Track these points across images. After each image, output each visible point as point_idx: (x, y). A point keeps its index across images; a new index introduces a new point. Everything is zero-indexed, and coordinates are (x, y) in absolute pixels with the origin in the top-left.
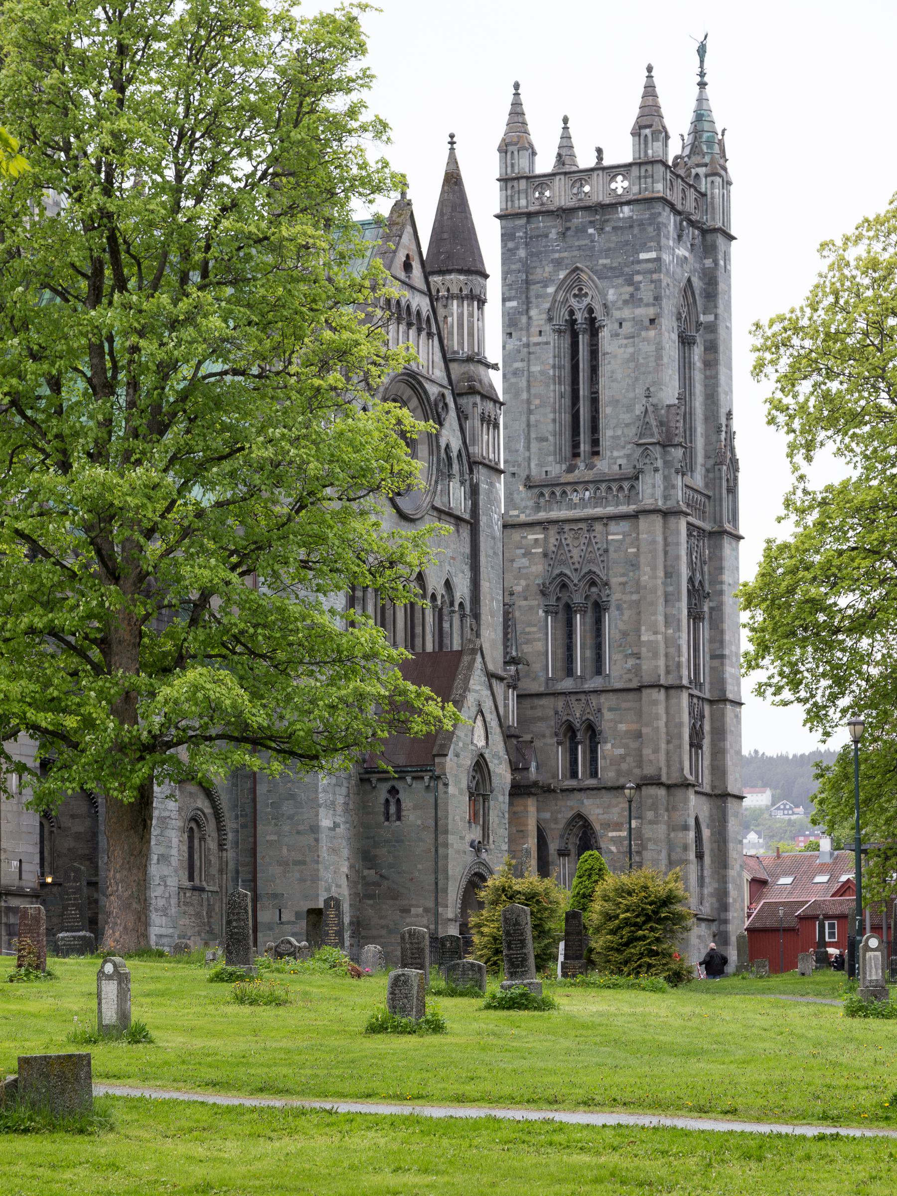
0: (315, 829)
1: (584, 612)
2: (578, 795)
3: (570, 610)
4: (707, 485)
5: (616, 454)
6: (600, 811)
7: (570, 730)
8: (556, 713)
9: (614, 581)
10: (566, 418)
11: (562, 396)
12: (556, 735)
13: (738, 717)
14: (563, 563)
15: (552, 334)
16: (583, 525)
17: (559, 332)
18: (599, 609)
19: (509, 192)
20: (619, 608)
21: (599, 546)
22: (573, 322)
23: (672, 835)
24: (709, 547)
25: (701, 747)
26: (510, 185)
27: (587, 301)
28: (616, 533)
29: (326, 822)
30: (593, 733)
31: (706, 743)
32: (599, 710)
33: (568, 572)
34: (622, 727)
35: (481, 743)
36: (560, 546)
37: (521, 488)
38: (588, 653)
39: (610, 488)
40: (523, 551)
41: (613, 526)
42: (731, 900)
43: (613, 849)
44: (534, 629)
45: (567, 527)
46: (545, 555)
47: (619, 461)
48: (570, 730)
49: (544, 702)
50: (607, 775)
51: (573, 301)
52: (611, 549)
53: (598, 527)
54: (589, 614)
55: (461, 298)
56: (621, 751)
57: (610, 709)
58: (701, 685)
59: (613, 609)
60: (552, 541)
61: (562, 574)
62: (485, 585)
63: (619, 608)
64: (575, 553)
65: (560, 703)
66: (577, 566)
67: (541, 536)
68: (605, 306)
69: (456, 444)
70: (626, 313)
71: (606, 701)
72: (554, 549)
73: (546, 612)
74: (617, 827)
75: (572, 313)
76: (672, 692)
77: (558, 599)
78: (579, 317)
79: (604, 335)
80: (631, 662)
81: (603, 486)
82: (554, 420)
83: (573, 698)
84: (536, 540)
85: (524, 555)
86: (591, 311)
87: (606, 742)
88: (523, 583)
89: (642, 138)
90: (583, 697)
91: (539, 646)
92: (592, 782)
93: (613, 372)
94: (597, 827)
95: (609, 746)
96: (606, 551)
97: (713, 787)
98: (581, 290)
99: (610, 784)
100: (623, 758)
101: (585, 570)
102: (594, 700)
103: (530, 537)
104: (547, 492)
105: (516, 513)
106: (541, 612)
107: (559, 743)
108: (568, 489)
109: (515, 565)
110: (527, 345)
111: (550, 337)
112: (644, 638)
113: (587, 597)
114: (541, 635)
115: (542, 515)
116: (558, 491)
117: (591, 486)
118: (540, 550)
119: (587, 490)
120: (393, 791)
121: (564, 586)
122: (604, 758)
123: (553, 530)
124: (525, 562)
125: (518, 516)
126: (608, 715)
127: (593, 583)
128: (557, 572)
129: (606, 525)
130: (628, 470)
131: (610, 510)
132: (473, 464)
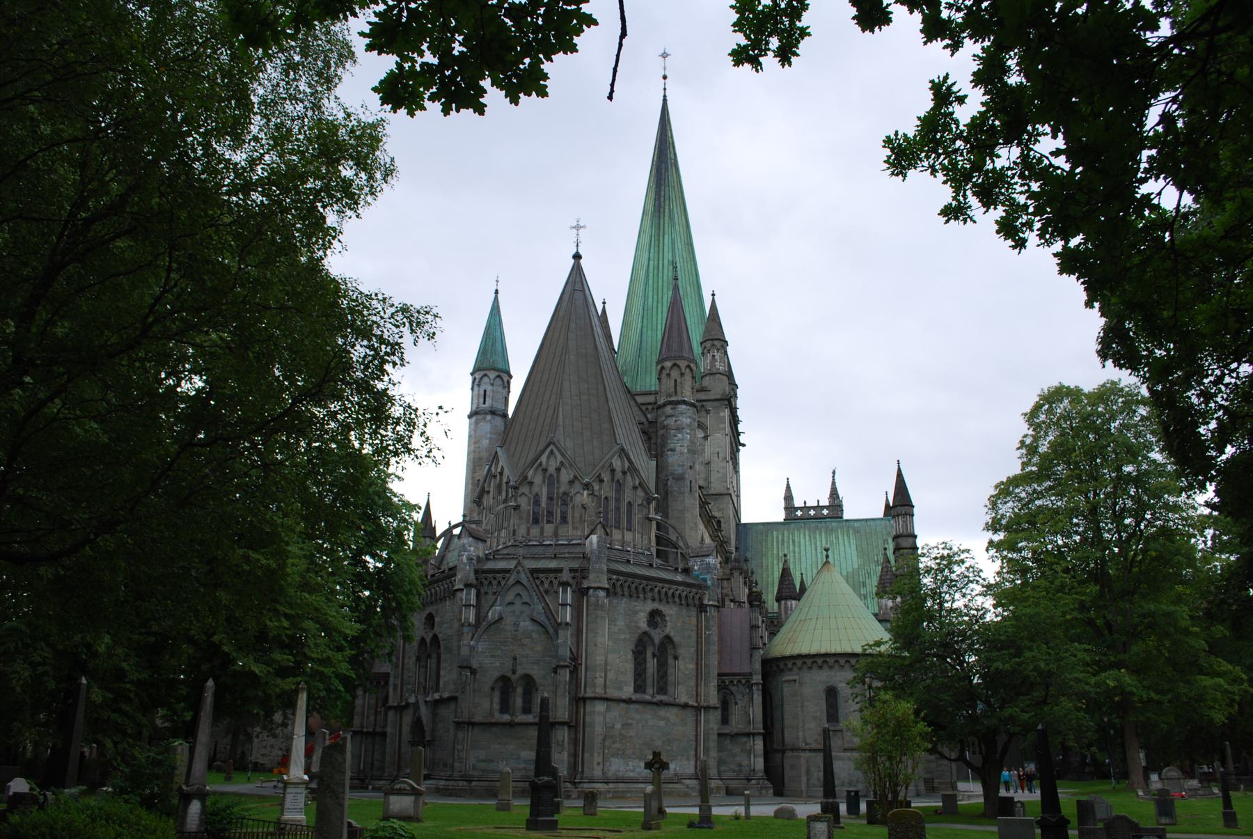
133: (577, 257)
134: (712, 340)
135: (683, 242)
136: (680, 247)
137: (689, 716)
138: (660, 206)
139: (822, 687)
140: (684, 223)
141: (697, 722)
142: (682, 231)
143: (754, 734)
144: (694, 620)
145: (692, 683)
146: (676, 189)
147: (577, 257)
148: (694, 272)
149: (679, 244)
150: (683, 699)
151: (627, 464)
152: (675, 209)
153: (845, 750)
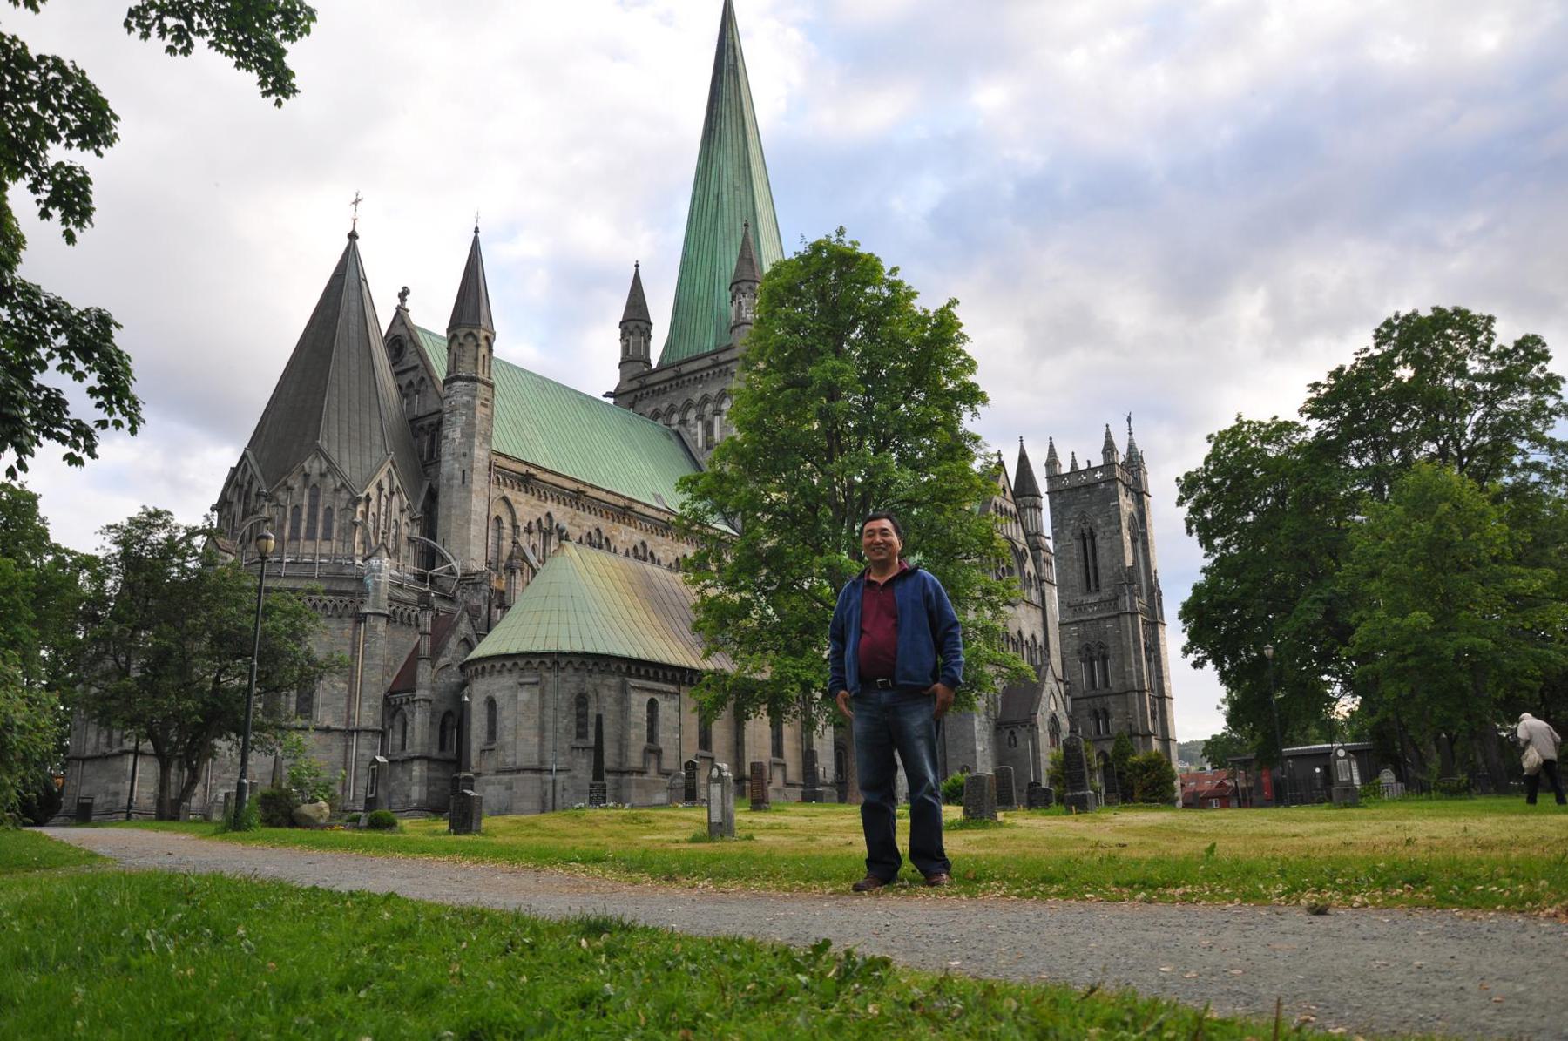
0: (974, 751)
29: (979, 748)
30: (1107, 715)
35: (1054, 708)
36: (1085, 631)
55: (1031, 508)
62: (1051, 637)
65: (1090, 701)
69: (1033, 572)
71: (1111, 699)
79: (1098, 538)
120: (1012, 733)
121: (1088, 649)
132: (1042, 581)
133: (353, 236)
134: (737, 283)
135: (736, 167)
136: (730, 173)
137: (336, 743)
138: (711, 129)
139: (483, 698)
140: (741, 142)
141: (347, 748)
142: (736, 153)
143: (411, 759)
144: (349, 632)
145: (343, 704)
146: (733, 102)
147: (353, 236)
148: (750, 201)
149: (730, 170)
150: (329, 721)
151: (325, 465)
152: (728, 127)
153: (498, 772)
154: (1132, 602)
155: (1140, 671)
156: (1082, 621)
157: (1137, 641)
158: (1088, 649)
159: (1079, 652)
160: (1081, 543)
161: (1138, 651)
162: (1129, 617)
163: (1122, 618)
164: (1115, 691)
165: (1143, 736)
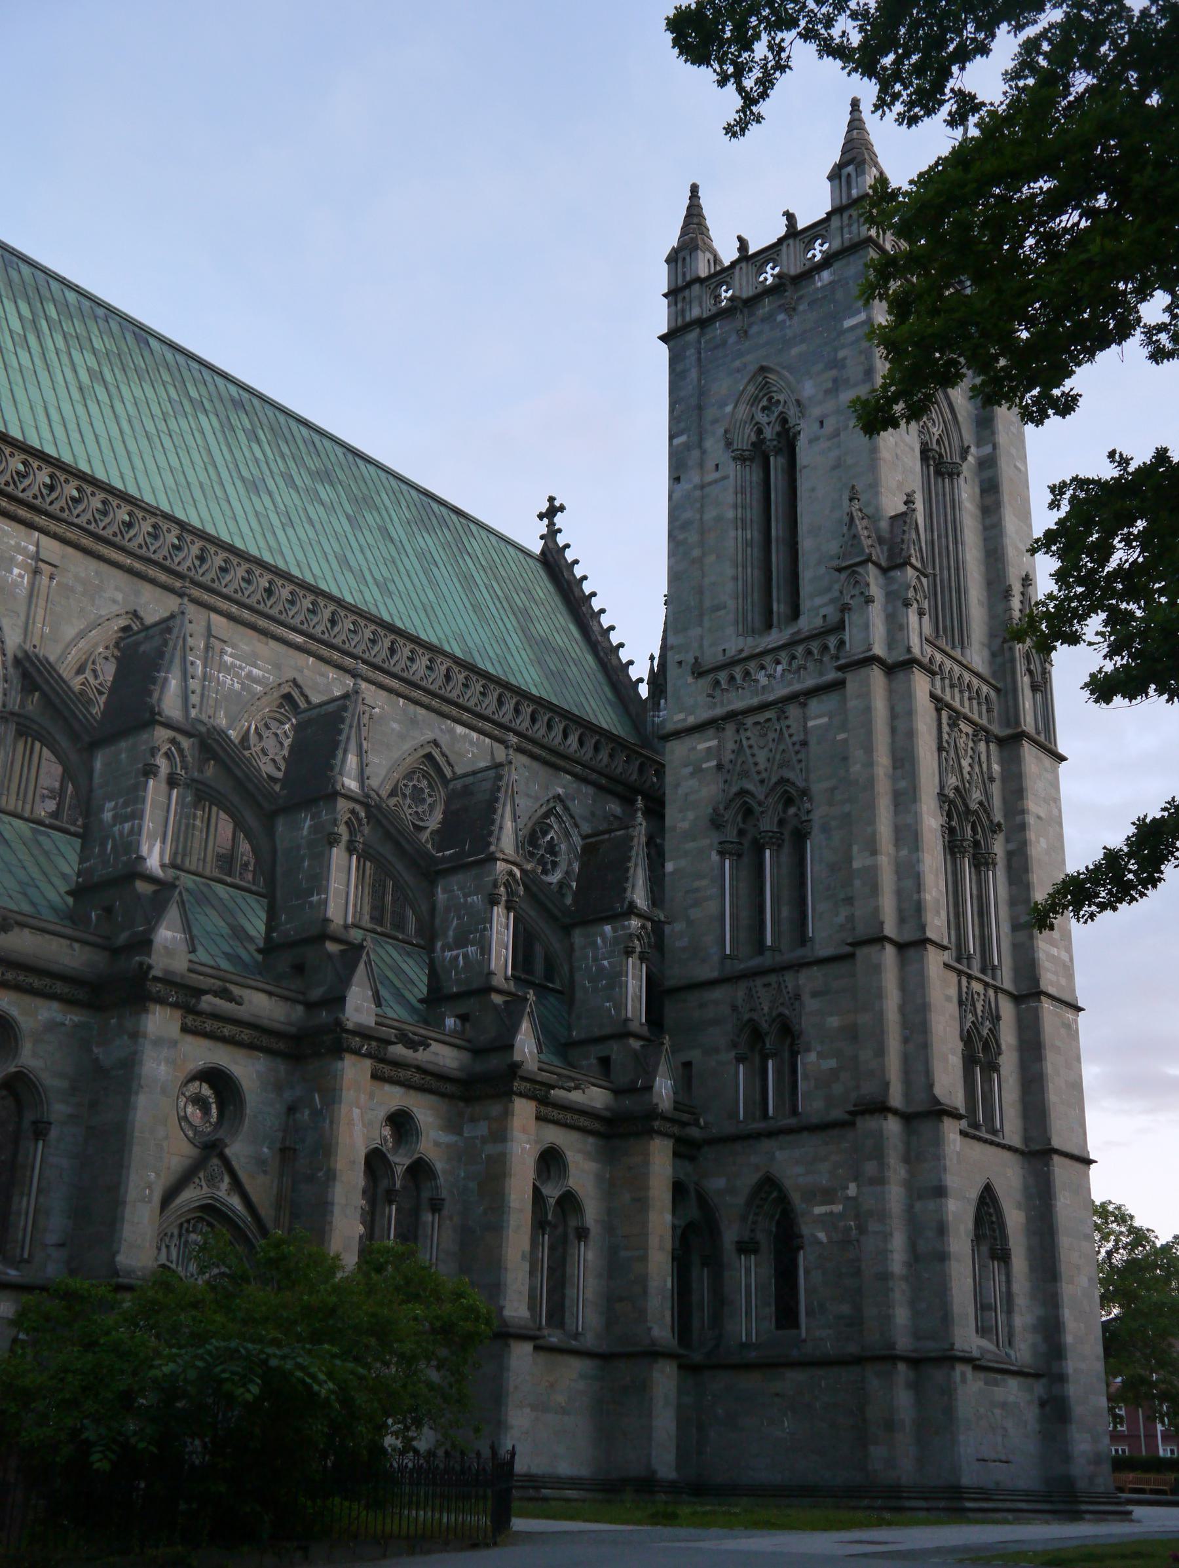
1: (778, 847)
2: (766, 1145)
3: (758, 850)
4: (994, 674)
5: (818, 601)
6: (800, 1170)
7: (757, 1035)
8: (734, 1008)
9: (818, 788)
10: (754, 574)
11: (747, 543)
12: (735, 1045)
13: (1072, 1033)
14: (745, 774)
15: (732, 464)
16: (768, 714)
17: (741, 459)
18: (800, 837)
19: (680, 306)
20: (825, 829)
21: (795, 738)
22: (763, 441)
23: (918, 1206)
24: (1002, 763)
25: (995, 1068)
26: (680, 297)
27: (777, 411)
28: (818, 715)
31: (1008, 1062)
32: (798, 997)
33: (750, 787)
34: (834, 1022)
36: (739, 751)
37: (690, 680)
38: (785, 912)
39: (809, 653)
40: (690, 769)
41: (814, 705)
42: (1069, 1339)
43: (822, 1236)
44: (704, 882)
45: (749, 721)
46: (719, 767)
47: (823, 611)
48: (757, 1035)
49: (718, 994)
50: (812, 1105)
51: (762, 418)
52: (813, 741)
53: (793, 711)
54: (786, 850)
56: (832, 1063)
57: (815, 994)
58: (994, 968)
59: (816, 831)
60: (730, 745)
61: (743, 792)
63: (825, 829)
64: (761, 756)
65: (740, 992)
66: (764, 775)
67: (714, 743)
68: (798, 402)
70: (830, 406)
71: (808, 980)
72: (732, 757)
73: (721, 853)
74: (828, 1196)
75: (760, 431)
76: (911, 953)
77: (741, 833)
78: (768, 433)
79: (802, 444)
80: (844, 913)
81: (800, 650)
82: (736, 579)
83: (759, 982)
84: (709, 748)
85: (692, 774)
86: (784, 420)
87: (808, 1050)
88: (691, 815)
89: (843, 179)
90: (772, 979)
91: (712, 907)
92: (792, 1121)
93: (813, 490)
94: (796, 1198)
95: (812, 1057)
96: (804, 743)
97: (1027, 1139)
98: (770, 399)
99: (815, 1120)
100: (834, 1074)
101: (774, 780)
102: (789, 979)
103: (701, 746)
104: (723, 676)
105: (681, 716)
106: (715, 857)
107: (740, 1059)
108: (752, 666)
109: (680, 791)
110: (702, 487)
111: (731, 469)
112: (856, 865)
113: (781, 822)
114: (714, 891)
115: (719, 711)
116: (738, 672)
117: (783, 656)
118: (714, 763)
119: (778, 663)
121: (748, 812)
122: (806, 1077)
123: (730, 729)
124: (693, 783)
125: (685, 720)
126: (811, 1004)
127: (789, 801)
128: (734, 789)
129: (804, 705)
130: (834, 618)
131: (810, 683)
154: (895, 626)
155: (910, 876)
156: (731, 716)
157: (904, 760)
158: (748, 812)
159: (716, 823)
160: (756, 476)
161: (905, 799)
162: (876, 675)
163: (853, 682)
164: (824, 951)
165: (908, 1118)
